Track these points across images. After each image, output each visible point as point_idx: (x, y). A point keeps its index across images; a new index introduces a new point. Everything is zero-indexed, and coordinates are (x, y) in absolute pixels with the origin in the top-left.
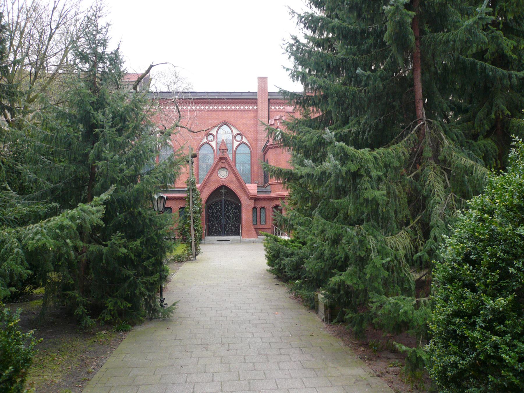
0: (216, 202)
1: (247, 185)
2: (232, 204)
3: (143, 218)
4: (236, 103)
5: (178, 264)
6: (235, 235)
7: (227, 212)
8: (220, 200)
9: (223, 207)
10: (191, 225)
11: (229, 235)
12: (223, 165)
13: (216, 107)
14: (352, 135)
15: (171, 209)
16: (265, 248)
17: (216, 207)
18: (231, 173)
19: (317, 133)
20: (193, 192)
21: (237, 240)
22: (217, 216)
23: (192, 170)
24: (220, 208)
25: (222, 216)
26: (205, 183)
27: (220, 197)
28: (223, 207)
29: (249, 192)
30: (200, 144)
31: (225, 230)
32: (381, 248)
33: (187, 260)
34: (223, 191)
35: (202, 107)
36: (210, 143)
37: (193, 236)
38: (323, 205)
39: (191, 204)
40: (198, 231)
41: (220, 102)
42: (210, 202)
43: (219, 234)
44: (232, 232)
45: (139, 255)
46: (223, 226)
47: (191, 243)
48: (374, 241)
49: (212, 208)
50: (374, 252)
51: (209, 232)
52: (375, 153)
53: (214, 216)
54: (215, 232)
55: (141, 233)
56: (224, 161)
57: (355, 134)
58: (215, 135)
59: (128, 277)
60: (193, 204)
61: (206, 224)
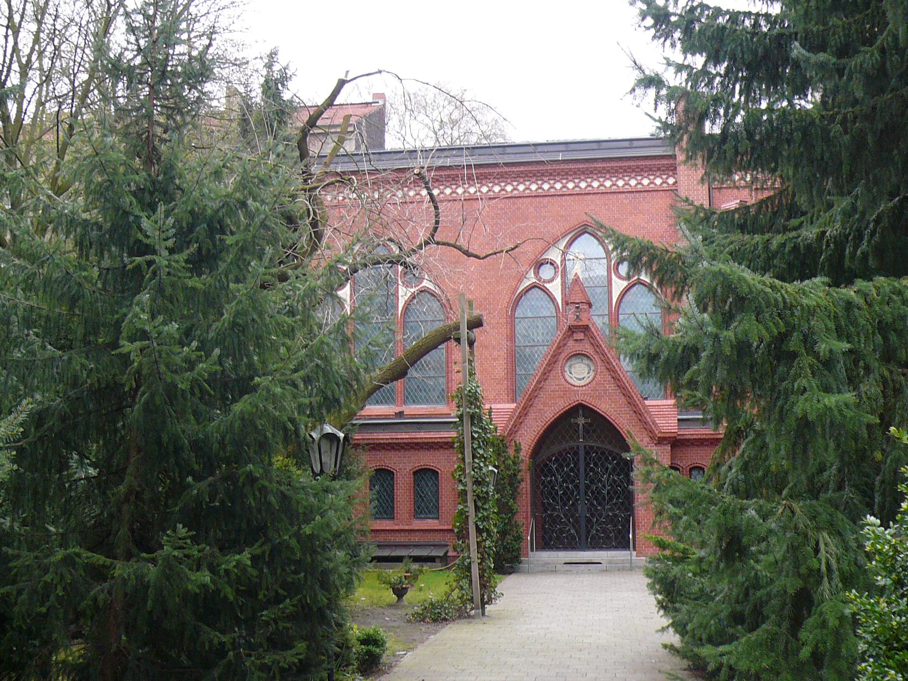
0: (560, 454)
1: (647, 402)
2: (607, 459)
3: (260, 490)
4: (617, 171)
5: (432, 627)
6: (616, 548)
7: (592, 482)
8: (572, 448)
9: (582, 470)
10: (467, 517)
11: (601, 548)
12: (579, 348)
13: (558, 186)
14: (828, 245)
15: (435, 473)
16: (649, 581)
17: (561, 466)
18: (601, 368)
19: (732, 243)
20: (473, 424)
21: (623, 562)
22: (565, 494)
23: (470, 362)
24: (572, 470)
25: (579, 494)
26: (530, 400)
27: (571, 437)
28: (582, 470)
29: (654, 422)
30: (516, 288)
31: (588, 532)
32: (854, 569)
33: (460, 617)
34: (581, 421)
35: (497, 189)
36: (547, 285)
37: (474, 547)
38: (753, 449)
39: (468, 459)
40: (489, 535)
41: (570, 170)
42: (544, 454)
43: (571, 545)
44: (608, 538)
45: (250, 591)
46: (583, 523)
47: (469, 568)
48: (833, 548)
49: (550, 470)
50: (830, 580)
51: (543, 538)
52: (849, 292)
53: (557, 493)
54: (558, 538)
55: (257, 532)
56: (581, 336)
57: (835, 243)
58: (559, 262)
59: (221, 651)
60: (474, 457)
61: (534, 515)
